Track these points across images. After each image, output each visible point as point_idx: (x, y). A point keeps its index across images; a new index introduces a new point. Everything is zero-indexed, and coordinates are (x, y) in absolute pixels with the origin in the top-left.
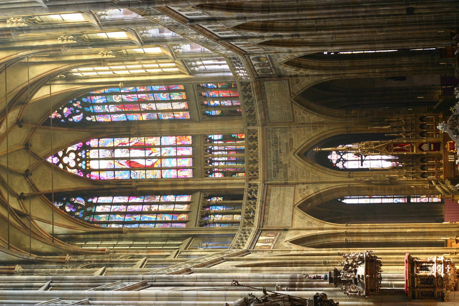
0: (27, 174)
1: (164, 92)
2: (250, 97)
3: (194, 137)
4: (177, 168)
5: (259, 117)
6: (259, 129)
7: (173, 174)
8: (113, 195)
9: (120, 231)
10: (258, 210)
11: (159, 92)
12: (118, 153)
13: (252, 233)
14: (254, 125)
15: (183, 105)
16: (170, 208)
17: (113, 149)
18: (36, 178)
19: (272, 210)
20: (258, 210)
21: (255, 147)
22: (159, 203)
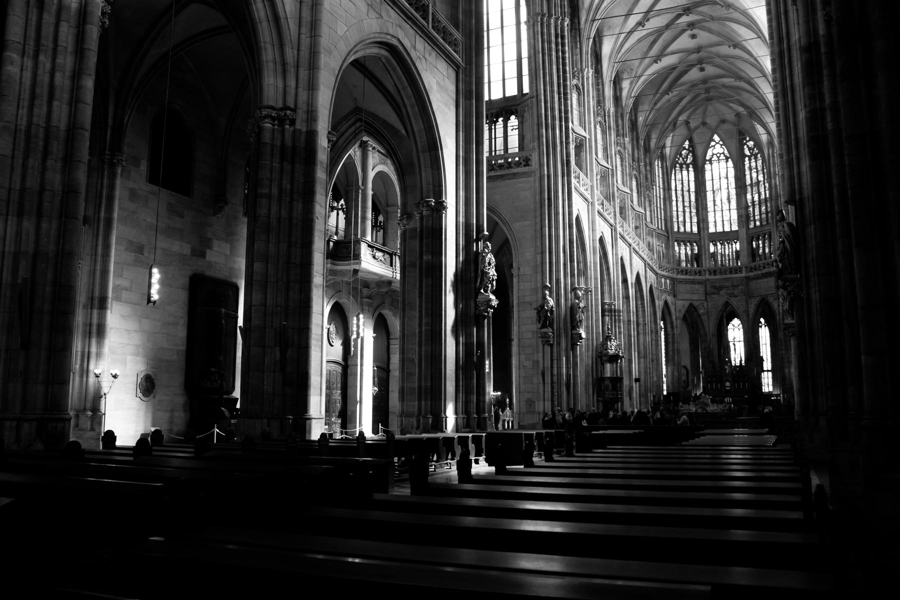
0: (704, 124)
1: (766, 209)
2: (764, 268)
3: (736, 231)
4: (715, 222)
5: (751, 274)
6: (744, 274)
7: (711, 219)
8: (695, 181)
9: (669, 189)
10: (688, 277)
11: (766, 206)
12: (724, 181)
13: (671, 275)
14: (746, 272)
15: (758, 223)
16: (688, 220)
17: (727, 178)
18: (702, 129)
19: (688, 286)
20: (688, 277)
21: (731, 273)
22: (691, 212)
